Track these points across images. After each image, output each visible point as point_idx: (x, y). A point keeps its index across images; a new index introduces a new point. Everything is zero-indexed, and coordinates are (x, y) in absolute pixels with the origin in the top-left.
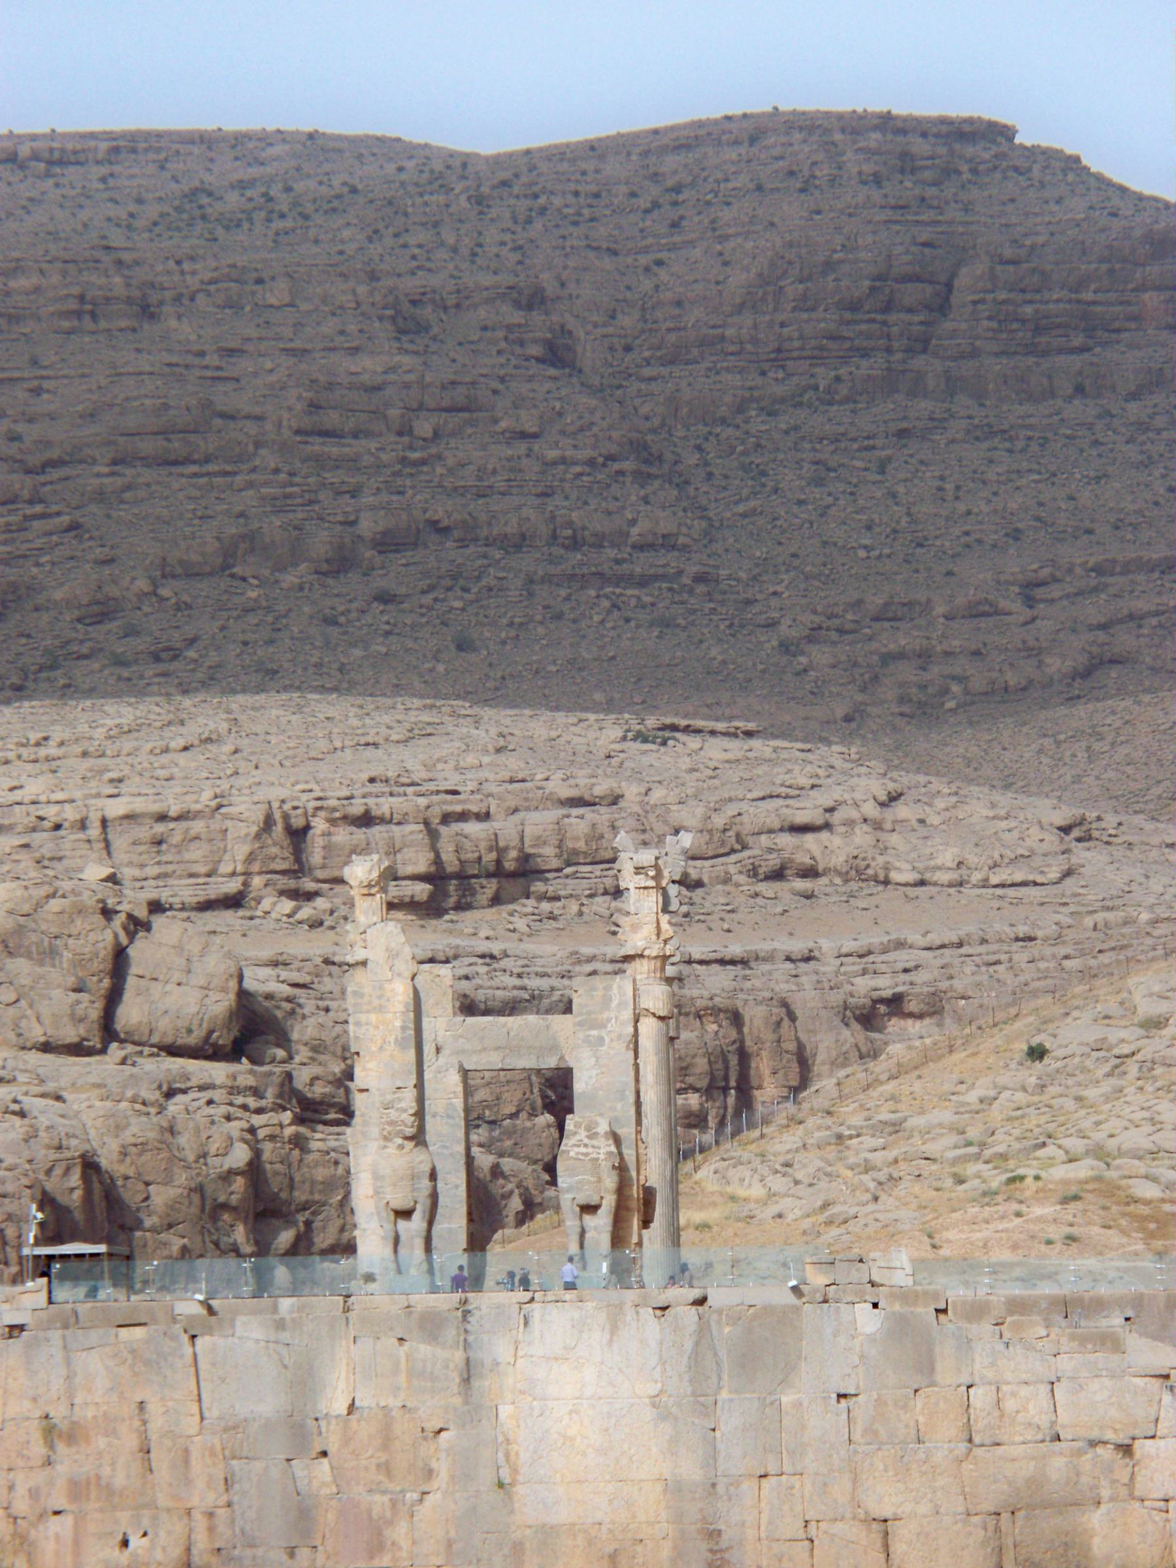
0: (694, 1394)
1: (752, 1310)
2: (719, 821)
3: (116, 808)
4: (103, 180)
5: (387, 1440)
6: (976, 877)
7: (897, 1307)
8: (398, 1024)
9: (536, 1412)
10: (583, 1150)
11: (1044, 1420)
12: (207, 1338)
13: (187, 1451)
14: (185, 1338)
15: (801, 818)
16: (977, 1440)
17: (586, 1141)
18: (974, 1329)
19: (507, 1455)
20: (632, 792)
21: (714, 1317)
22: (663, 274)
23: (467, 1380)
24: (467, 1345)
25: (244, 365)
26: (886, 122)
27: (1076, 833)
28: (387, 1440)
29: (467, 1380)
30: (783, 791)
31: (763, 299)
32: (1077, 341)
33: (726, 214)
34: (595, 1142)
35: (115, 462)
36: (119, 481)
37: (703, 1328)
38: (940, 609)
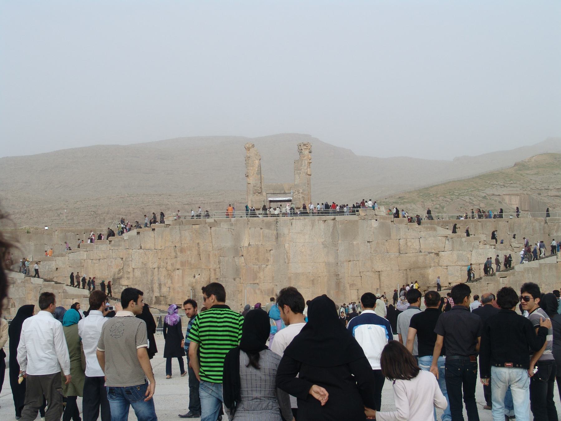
0: (332, 242)
3: (212, 201)
5: (258, 252)
7: (382, 221)
8: (257, 169)
9: (294, 246)
11: (418, 247)
12: (214, 228)
13: (209, 255)
14: (209, 228)
16: (401, 253)
18: (400, 226)
19: (287, 256)
21: (337, 223)
23: (277, 238)
24: (277, 230)
28: (258, 252)
29: (277, 238)
34: (299, 194)
37: (334, 226)
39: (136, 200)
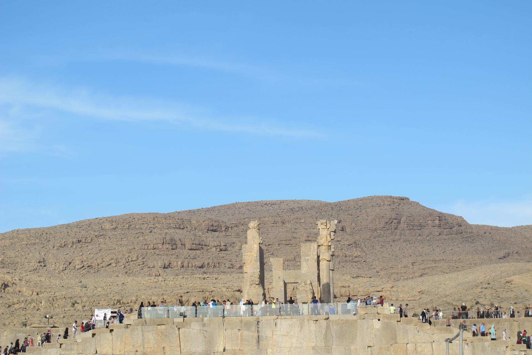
1: (342, 321)
2: (365, 290)
4: (279, 207)
6: (406, 299)
7: (386, 320)
10: (303, 288)
15: (378, 290)
17: (304, 286)
20: (352, 286)
22: (359, 218)
25: (297, 231)
26: (391, 197)
27: (421, 293)
30: (375, 286)
31: (373, 222)
32: (419, 228)
33: (368, 210)
34: (306, 286)
35: (279, 245)
36: (279, 247)
38: (400, 266)
39: (172, 285)
